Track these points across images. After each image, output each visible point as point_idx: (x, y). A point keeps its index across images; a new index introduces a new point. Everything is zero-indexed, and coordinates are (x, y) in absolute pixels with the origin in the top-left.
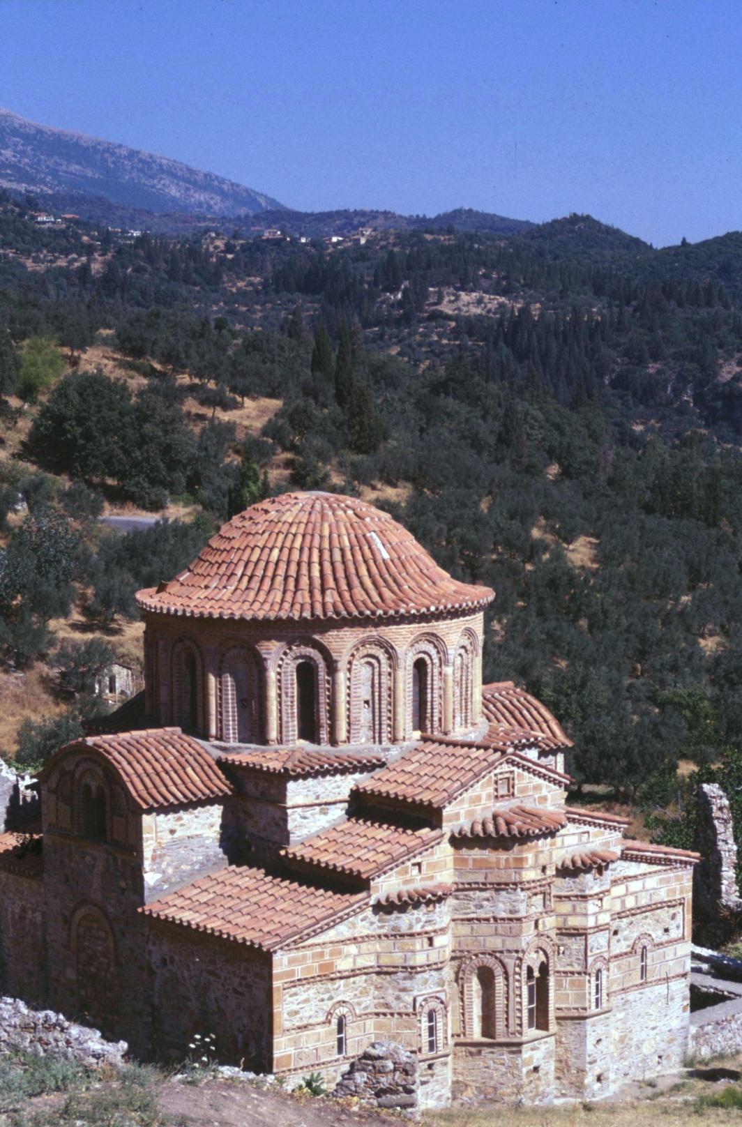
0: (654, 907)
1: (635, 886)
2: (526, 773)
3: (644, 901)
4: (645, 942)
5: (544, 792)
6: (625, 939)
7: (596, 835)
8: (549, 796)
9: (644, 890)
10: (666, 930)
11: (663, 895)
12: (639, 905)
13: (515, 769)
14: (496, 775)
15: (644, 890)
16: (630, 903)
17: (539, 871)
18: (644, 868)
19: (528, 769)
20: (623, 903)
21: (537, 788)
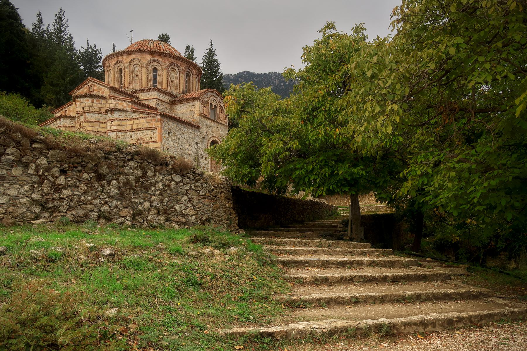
0: (144, 129)
1: (136, 121)
2: (97, 85)
3: (140, 127)
4: (141, 140)
5: (103, 90)
6: (135, 139)
7: (120, 104)
8: (105, 92)
9: (140, 123)
10: (151, 138)
11: (147, 125)
12: (138, 128)
13: (94, 84)
14: (88, 86)
15: (140, 123)
16: (135, 127)
17: (81, 108)
18: (141, 115)
19: (97, 83)
20: (132, 126)
21: (101, 89)
